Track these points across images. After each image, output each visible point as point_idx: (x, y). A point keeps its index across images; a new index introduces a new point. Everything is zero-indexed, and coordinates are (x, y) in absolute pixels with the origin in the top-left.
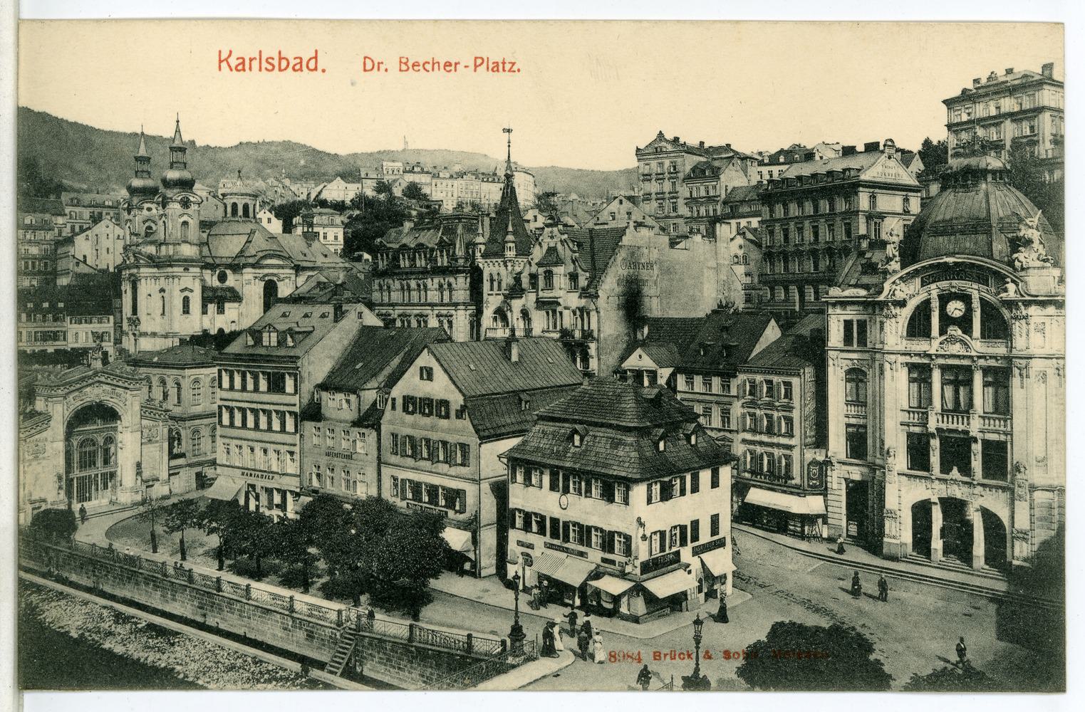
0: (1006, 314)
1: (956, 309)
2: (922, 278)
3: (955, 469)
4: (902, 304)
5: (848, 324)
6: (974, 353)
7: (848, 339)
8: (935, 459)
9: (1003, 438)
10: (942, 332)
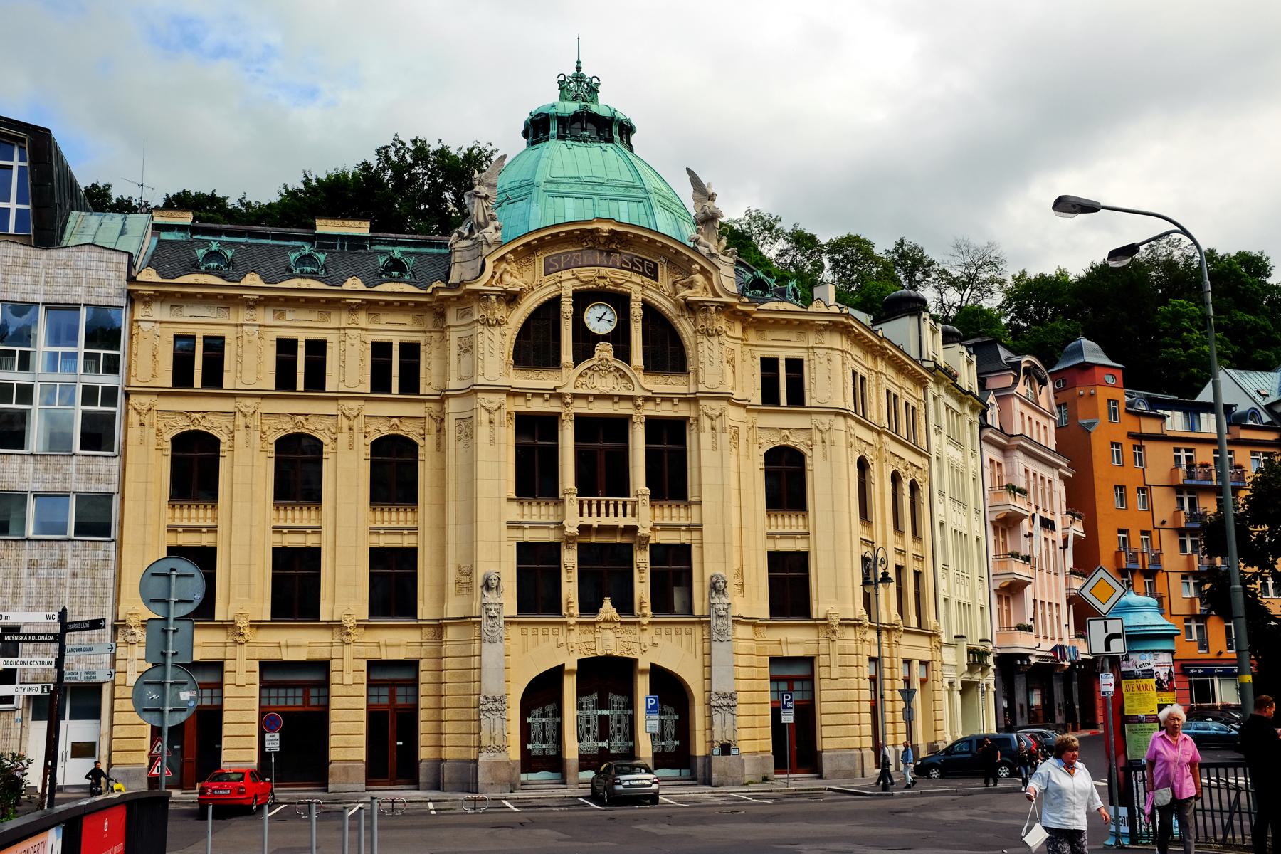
0: (685, 328)
3: (607, 603)
4: (512, 299)
5: (380, 351)
6: (638, 392)
7: (380, 381)
8: (570, 589)
9: (684, 538)
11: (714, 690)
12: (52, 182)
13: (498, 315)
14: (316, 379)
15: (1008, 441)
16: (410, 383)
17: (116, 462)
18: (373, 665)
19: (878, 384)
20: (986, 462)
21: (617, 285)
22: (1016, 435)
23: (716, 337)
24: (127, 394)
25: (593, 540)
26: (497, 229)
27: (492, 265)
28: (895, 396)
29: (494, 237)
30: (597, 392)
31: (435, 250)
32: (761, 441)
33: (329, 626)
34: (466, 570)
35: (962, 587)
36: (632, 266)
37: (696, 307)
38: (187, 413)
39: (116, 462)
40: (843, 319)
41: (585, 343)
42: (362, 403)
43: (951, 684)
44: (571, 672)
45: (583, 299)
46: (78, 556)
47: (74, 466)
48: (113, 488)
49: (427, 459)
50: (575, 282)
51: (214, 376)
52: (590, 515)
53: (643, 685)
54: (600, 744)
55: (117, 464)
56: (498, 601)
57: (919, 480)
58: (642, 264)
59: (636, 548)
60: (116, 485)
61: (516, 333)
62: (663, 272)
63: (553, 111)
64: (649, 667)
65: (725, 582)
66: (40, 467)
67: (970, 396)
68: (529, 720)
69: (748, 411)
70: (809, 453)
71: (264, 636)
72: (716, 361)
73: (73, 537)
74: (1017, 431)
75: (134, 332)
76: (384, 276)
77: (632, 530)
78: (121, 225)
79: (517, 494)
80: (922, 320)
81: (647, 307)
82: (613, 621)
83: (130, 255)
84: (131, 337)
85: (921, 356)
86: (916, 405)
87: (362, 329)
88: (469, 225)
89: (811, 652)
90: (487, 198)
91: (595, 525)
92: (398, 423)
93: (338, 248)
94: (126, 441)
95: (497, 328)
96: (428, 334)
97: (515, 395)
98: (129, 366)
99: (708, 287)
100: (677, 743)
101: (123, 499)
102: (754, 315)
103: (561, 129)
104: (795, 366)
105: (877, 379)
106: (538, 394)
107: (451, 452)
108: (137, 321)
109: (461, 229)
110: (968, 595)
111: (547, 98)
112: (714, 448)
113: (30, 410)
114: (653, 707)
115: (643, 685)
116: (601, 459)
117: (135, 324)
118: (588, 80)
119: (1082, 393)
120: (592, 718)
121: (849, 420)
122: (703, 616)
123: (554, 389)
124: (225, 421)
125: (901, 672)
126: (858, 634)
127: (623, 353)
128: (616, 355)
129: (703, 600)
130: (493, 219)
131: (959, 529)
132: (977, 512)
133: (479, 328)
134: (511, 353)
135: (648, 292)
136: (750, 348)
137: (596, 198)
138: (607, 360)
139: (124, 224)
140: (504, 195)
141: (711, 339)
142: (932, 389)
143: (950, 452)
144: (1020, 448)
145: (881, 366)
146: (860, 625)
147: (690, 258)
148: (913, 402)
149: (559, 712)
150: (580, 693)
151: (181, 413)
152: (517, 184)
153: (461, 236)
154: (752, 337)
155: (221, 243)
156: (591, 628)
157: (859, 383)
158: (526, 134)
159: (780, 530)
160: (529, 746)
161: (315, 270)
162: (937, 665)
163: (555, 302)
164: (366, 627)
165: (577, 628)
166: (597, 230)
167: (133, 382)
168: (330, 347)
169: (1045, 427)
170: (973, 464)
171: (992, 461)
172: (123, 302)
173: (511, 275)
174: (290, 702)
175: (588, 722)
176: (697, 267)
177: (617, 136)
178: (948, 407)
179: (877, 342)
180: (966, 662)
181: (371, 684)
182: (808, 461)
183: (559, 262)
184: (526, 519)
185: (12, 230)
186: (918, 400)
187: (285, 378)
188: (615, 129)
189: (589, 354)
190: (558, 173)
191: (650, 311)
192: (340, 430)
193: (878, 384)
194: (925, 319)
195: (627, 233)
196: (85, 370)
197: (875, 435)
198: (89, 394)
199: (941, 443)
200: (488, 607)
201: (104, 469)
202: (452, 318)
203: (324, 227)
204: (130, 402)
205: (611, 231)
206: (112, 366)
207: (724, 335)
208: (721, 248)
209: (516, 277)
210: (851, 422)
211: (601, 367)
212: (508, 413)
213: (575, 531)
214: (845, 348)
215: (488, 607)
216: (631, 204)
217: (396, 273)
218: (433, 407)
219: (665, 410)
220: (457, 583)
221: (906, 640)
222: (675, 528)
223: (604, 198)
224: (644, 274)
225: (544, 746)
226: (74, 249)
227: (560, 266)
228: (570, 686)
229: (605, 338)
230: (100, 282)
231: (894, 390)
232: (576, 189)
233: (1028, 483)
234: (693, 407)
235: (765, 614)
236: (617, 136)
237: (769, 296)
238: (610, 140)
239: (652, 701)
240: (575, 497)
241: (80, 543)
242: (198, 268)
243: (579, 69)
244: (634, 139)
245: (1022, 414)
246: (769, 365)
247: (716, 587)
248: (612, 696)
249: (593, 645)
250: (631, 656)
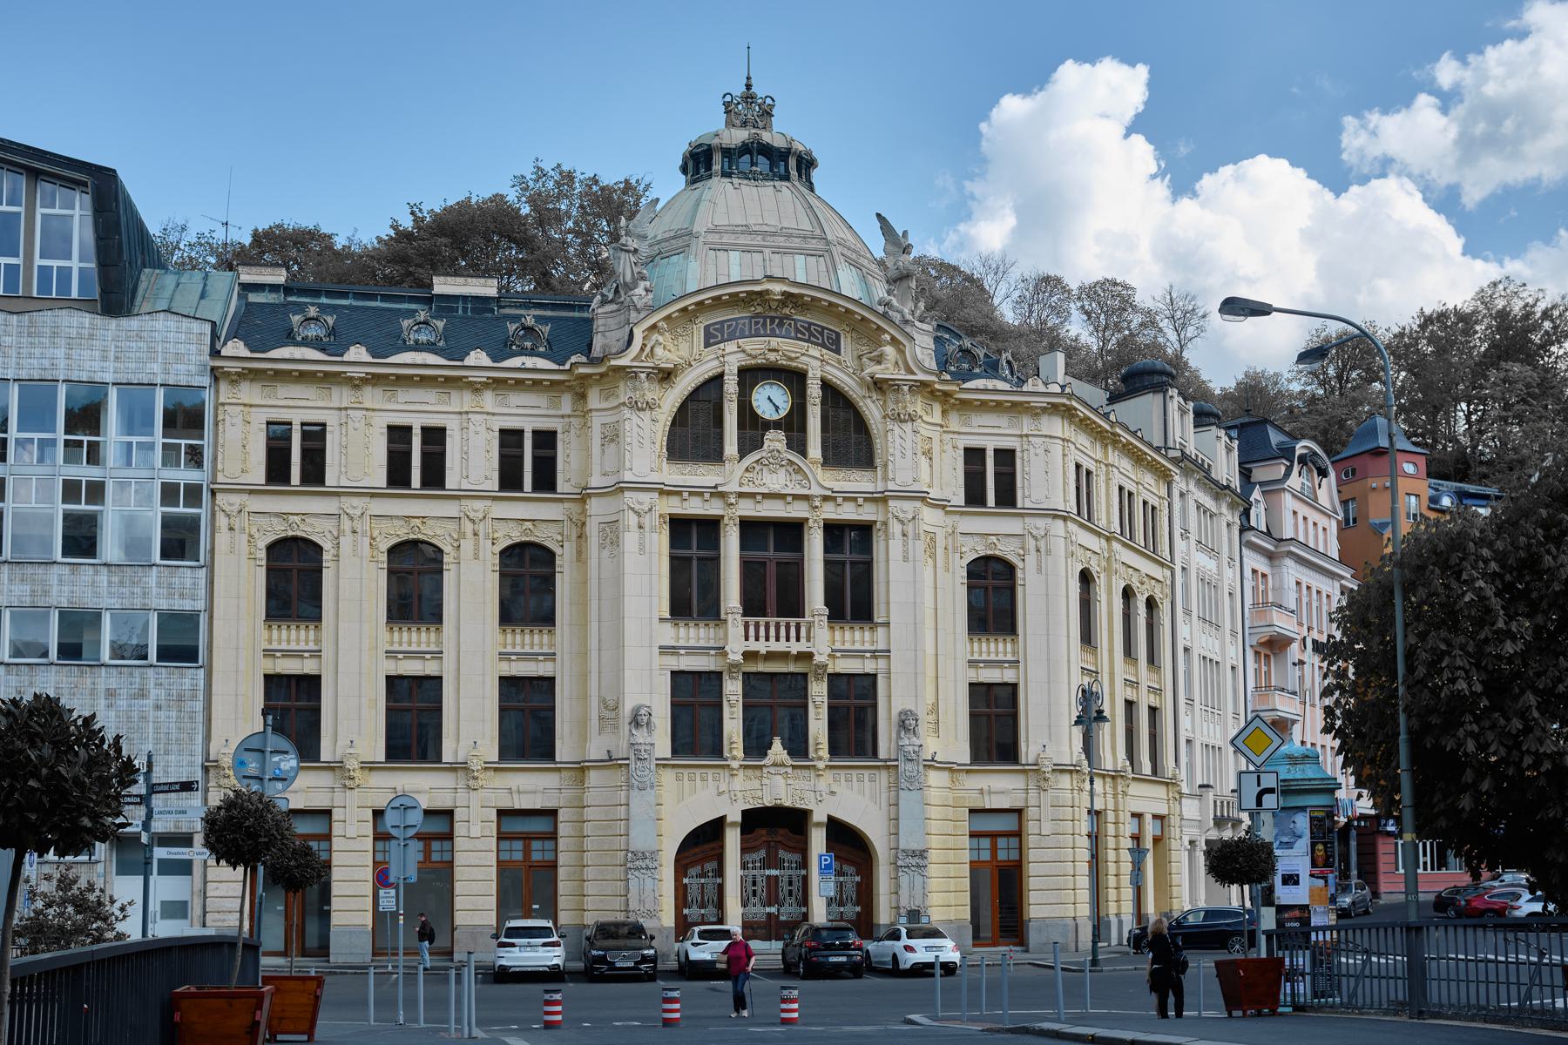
0: (872, 410)
2: (707, 328)
3: (777, 744)
4: (666, 376)
5: (510, 439)
6: (816, 491)
7: (510, 479)
8: (733, 726)
9: (869, 666)
11: (901, 847)
12: (120, 234)
13: (649, 397)
14: (434, 475)
15: (1276, 547)
16: (546, 480)
17: (202, 573)
18: (502, 813)
19: (1108, 480)
20: (1248, 574)
21: (790, 359)
22: (1286, 540)
23: (910, 424)
24: (213, 493)
25: (762, 667)
26: (647, 290)
27: (641, 336)
28: (1130, 494)
29: (645, 300)
30: (766, 491)
31: (576, 314)
32: (964, 549)
33: (453, 768)
34: (611, 704)
35: (1211, 725)
36: (809, 334)
37: (885, 387)
38: (282, 515)
39: (202, 573)
40: (1064, 401)
41: (753, 428)
42: (488, 503)
43: (1192, 843)
44: (733, 824)
45: (751, 376)
46: (161, 684)
47: (154, 578)
48: (200, 605)
49: (566, 570)
50: (741, 356)
51: (314, 472)
52: (757, 639)
53: (818, 840)
54: (768, 910)
55: (204, 576)
56: (649, 740)
57: (1158, 596)
58: (822, 334)
59: (811, 678)
60: (203, 601)
61: (670, 419)
62: (846, 344)
63: (716, 141)
64: (826, 820)
65: (917, 720)
66: (115, 579)
67: (1227, 491)
68: (686, 881)
69: (947, 513)
70: (1020, 565)
71: (377, 779)
72: (909, 453)
73: (155, 663)
74: (1288, 533)
75: (220, 418)
76: (514, 347)
77: (806, 657)
78: (202, 285)
79: (671, 614)
80: (1168, 398)
81: (826, 386)
82: (783, 765)
83: (213, 323)
84: (216, 424)
85: (1166, 442)
86: (1157, 505)
87: (488, 413)
88: (615, 285)
89: (1019, 804)
90: (636, 251)
91: (763, 651)
92: (531, 527)
93: (460, 312)
94: (213, 549)
95: (648, 412)
96: (566, 420)
97: (669, 493)
98: (215, 458)
99: (900, 362)
100: (858, 909)
101: (211, 617)
102: (957, 396)
103: (726, 165)
104: (1006, 457)
105: (1107, 473)
106: (696, 493)
107: (593, 563)
108: (223, 404)
109: (604, 291)
110: (1218, 736)
111: (711, 124)
112: (906, 559)
113: (102, 511)
114: (828, 867)
115: (818, 840)
116: (772, 570)
117: (220, 408)
118: (760, 101)
119: (1374, 485)
120: (759, 879)
121: (1069, 524)
122: (890, 760)
123: (715, 487)
124: (329, 525)
125: (1129, 828)
126: (1075, 782)
127: (798, 444)
128: (789, 446)
129: (890, 743)
130: (643, 278)
131: (1209, 656)
132: (1234, 633)
133: (627, 412)
134: (665, 443)
135: (828, 368)
136: (952, 436)
137: (767, 251)
138: (778, 451)
139: (205, 285)
140: (656, 248)
141: (904, 426)
142: (1180, 483)
143: (1201, 561)
144: (1291, 554)
145: (1113, 457)
146: (1078, 771)
147: (879, 327)
148: (1153, 501)
149: (720, 872)
150: (744, 850)
151: (278, 515)
152: (672, 234)
153: (604, 302)
154: (954, 422)
155: (320, 306)
156: (758, 773)
157: (1084, 478)
158: (684, 170)
160: (686, 911)
161: (432, 340)
162: (1174, 821)
163: (718, 379)
164: (496, 769)
165: (741, 773)
167: (220, 478)
168: (451, 436)
169: (1324, 529)
170: (1230, 575)
171: (1254, 571)
172: (206, 381)
173: (664, 348)
175: (754, 883)
176: (888, 337)
177: (794, 173)
178: (1199, 506)
179: (1108, 428)
180: (1212, 816)
181: (501, 837)
182: (1019, 574)
183: (721, 331)
184: (682, 643)
185: (75, 294)
186: (1160, 497)
187: (398, 474)
188: (792, 162)
189: (757, 444)
190: (721, 220)
191: (831, 391)
193: (1108, 480)
194: (1172, 397)
195: (802, 296)
196: (164, 464)
197: (1103, 542)
198: (169, 493)
199: (1188, 550)
200: (636, 747)
201: (188, 583)
202: (594, 399)
203: (443, 286)
204: (217, 502)
205: (784, 293)
206: (195, 457)
207: (919, 421)
208: (918, 313)
209: (670, 351)
210: (1072, 526)
211: (771, 460)
212: (661, 516)
213: (739, 658)
214: (1066, 436)
215: (636, 747)
216: (809, 258)
217: (528, 344)
218: (575, 508)
219: (848, 513)
220: (601, 718)
221: (1135, 789)
222: (859, 654)
223: (778, 250)
224: (823, 345)
225: (703, 911)
226: (147, 317)
227: (723, 335)
228: (733, 839)
229: (777, 425)
230: (179, 357)
231: (1130, 486)
232: (743, 240)
233: (1299, 600)
234: (881, 507)
235: (965, 757)
236: (794, 173)
237: (977, 370)
238: (786, 178)
239: (826, 860)
240: (739, 617)
241: (164, 670)
242: (294, 338)
243: (748, 87)
244: (816, 175)
245: (1295, 513)
246: (974, 456)
247: (906, 723)
248: (782, 854)
249: (759, 793)
250: (804, 807)
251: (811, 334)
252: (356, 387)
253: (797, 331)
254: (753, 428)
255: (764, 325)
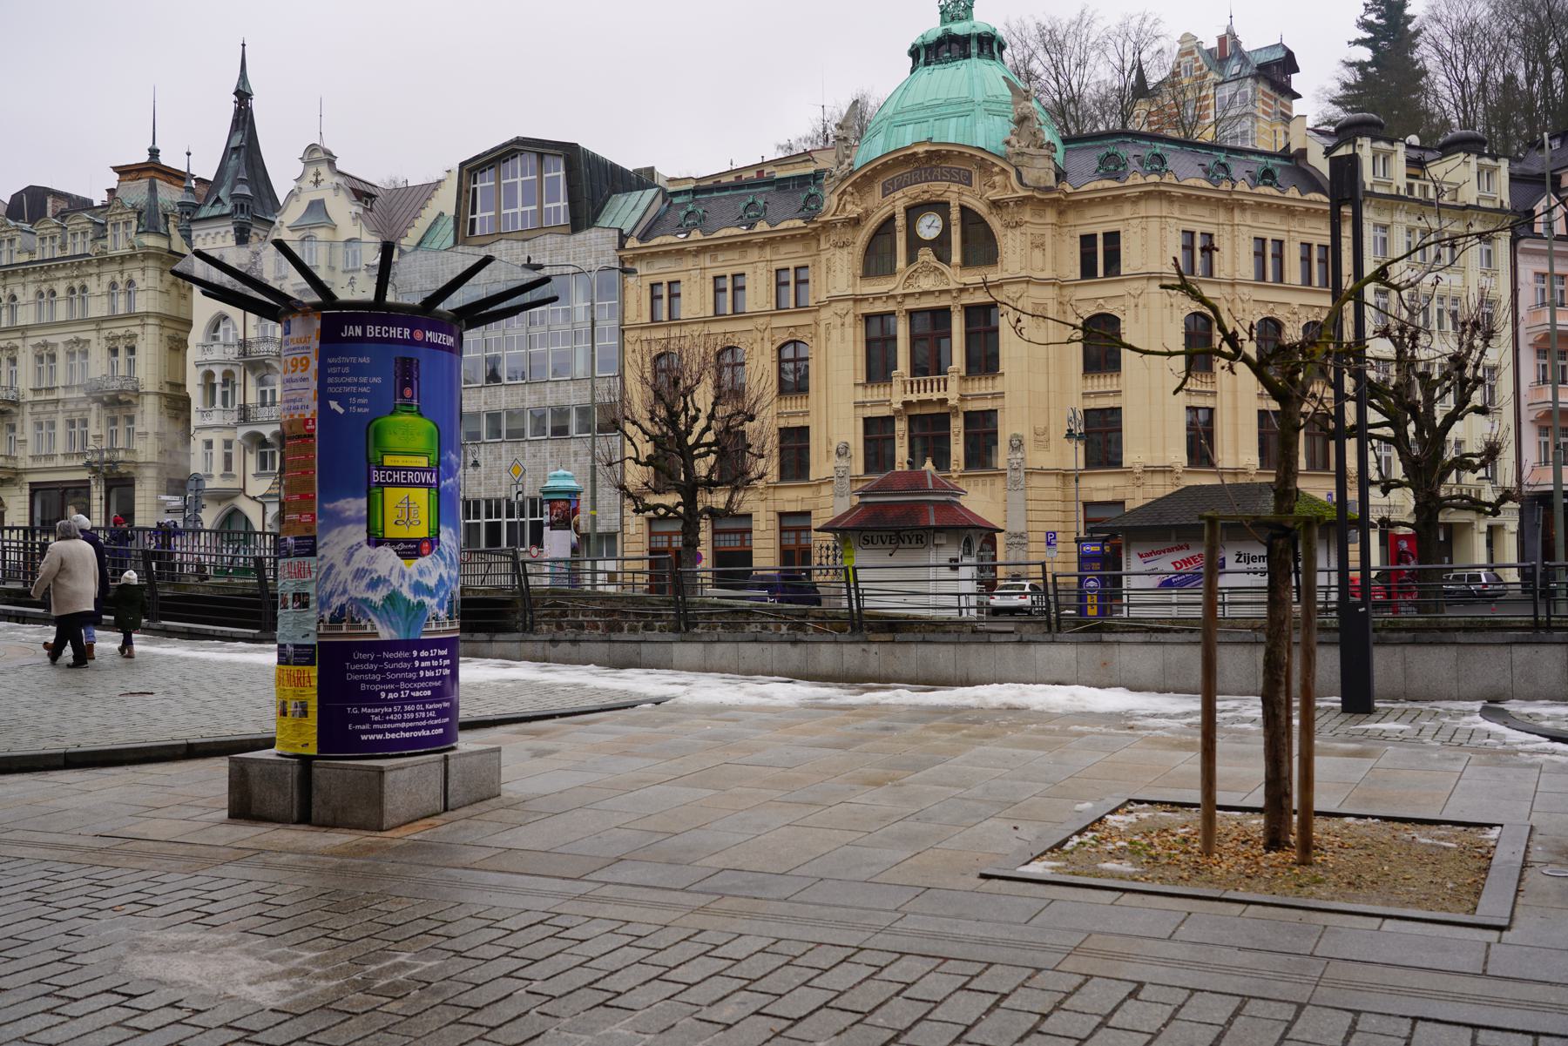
0: (995, 223)
1: (929, 227)
2: (883, 184)
4: (856, 222)
6: (953, 286)
10: (911, 258)
25: (918, 411)
45: (914, 211)
50: (906, 199)
77: (943, 401)
81: (964, 209)
97: (861, 300)
106: (877, 297)
127: (943, 257)
130: (848, 157)
137: (931, 120)
159: (1096, 390)
163: (892, 218)
166: (915, 154)
174: (733, 544)
181: (782, 530)
183: (892, 184)
184: (869, 399)
192: (755, 341)
205: (927, 152)
213: (899, 406)
247: (1017, 445)
251: (952, 175)
252: (696, 256)
253: (942, 175)
254: (914, 243)
255: (920, 176)
